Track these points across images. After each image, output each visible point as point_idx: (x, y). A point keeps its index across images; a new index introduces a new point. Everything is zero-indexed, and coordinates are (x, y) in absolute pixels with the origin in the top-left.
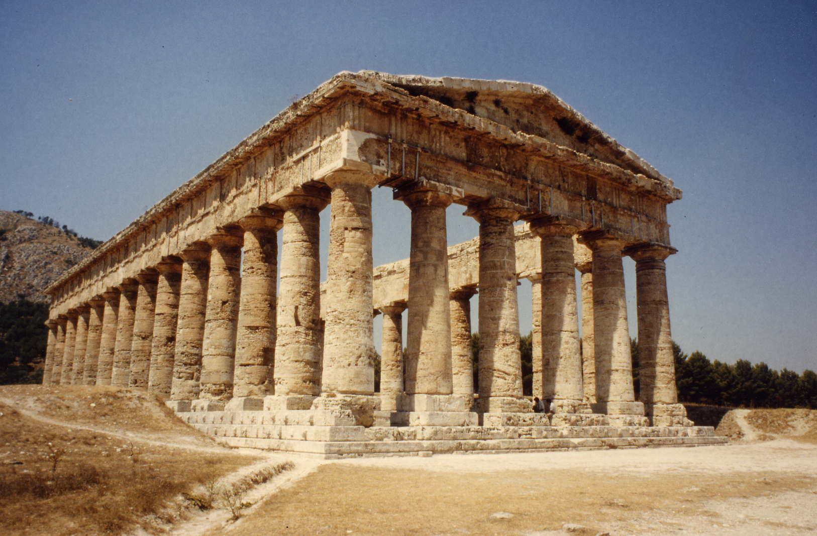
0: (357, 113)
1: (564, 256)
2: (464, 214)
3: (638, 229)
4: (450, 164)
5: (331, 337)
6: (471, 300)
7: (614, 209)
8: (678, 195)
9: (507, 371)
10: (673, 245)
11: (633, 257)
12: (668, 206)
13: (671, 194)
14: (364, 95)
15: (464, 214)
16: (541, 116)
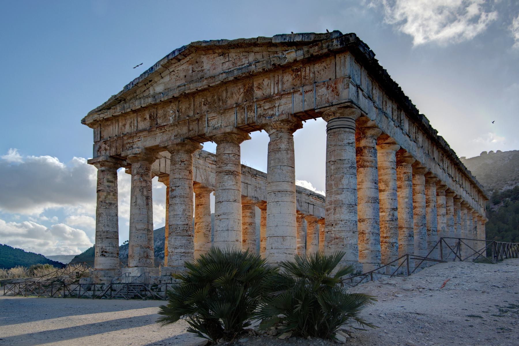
7: (269, 99)
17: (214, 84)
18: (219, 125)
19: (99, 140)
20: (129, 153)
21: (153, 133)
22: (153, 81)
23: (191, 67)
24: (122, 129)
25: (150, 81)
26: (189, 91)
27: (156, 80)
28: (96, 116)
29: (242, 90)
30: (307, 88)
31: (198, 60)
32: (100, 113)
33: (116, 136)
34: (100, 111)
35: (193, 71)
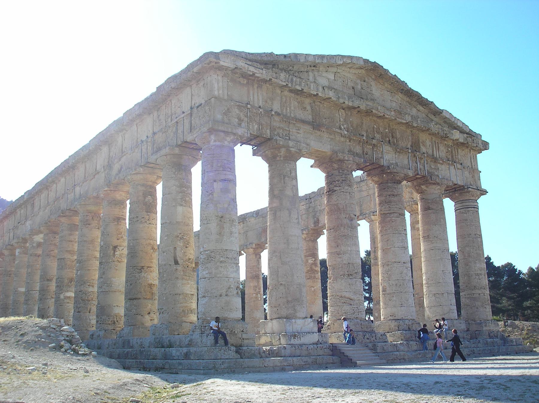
0: (221, 84)
1: (395, 199)
2: (312, 167)
3: (455, 176)
4: (299, 125)
5: (204, 273)
6: (319, 240)
7: (435, 160)
8: (485, 146)
9: (352, 297)
10: (484, 187)
11: (452, 199)
12: (479, 156)
13: (481, 146)
14: (227, 68)
15: (312, 167)
16: (373, 83)
17: (400, 121)
18: (394, 162)
19: (226, 97)
20: (291, 143)
21: (319, 133)
22: (317, 68)
23: (359, 81)
24: (266, 102)
25: (314, 66)
26: (376, 112)
27: (321, 69)
28: (241, 64)
29: (410, 138)
30: (459, 166)
31: (366, 79)
32: (250, 63)
33: (260, 107)
34: (250, 60)
35: (362, 88)
